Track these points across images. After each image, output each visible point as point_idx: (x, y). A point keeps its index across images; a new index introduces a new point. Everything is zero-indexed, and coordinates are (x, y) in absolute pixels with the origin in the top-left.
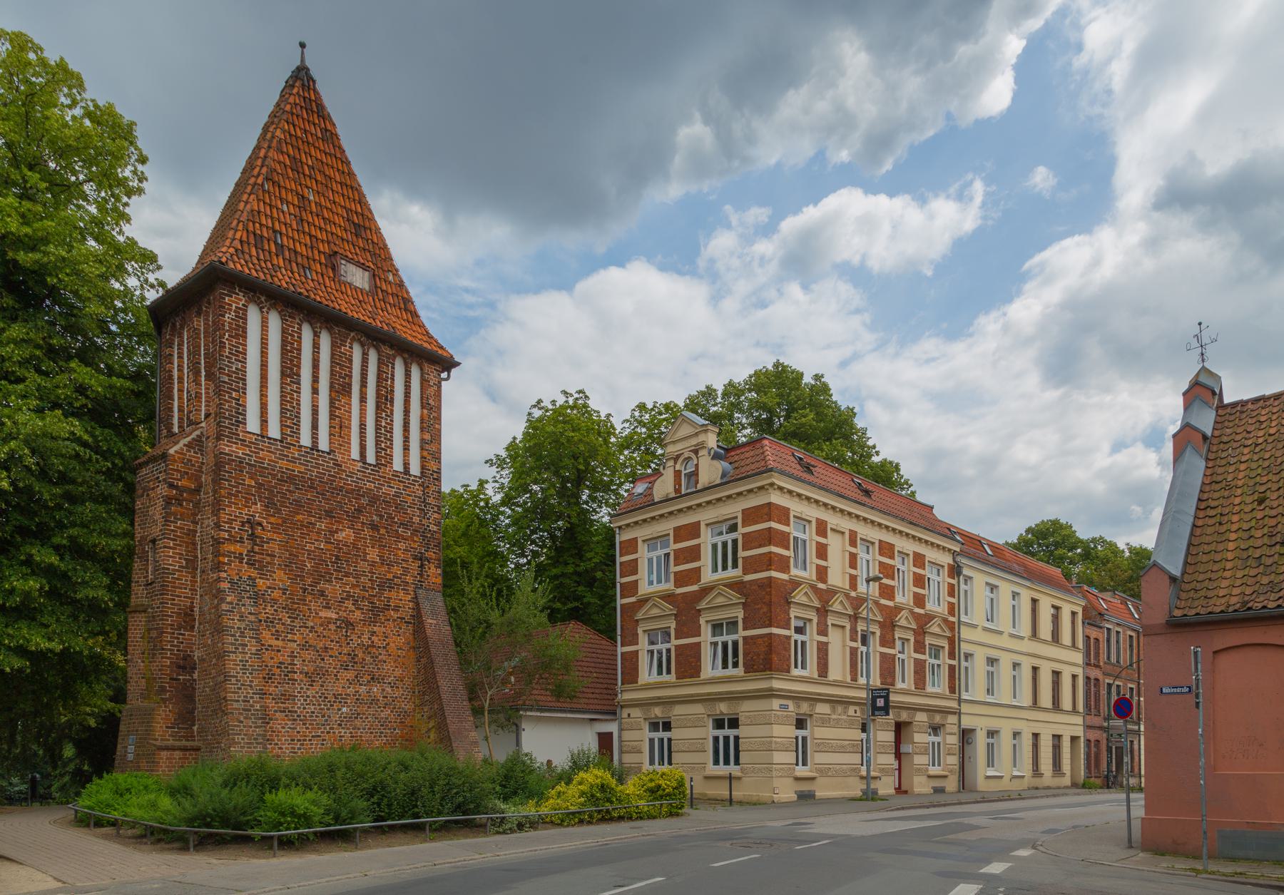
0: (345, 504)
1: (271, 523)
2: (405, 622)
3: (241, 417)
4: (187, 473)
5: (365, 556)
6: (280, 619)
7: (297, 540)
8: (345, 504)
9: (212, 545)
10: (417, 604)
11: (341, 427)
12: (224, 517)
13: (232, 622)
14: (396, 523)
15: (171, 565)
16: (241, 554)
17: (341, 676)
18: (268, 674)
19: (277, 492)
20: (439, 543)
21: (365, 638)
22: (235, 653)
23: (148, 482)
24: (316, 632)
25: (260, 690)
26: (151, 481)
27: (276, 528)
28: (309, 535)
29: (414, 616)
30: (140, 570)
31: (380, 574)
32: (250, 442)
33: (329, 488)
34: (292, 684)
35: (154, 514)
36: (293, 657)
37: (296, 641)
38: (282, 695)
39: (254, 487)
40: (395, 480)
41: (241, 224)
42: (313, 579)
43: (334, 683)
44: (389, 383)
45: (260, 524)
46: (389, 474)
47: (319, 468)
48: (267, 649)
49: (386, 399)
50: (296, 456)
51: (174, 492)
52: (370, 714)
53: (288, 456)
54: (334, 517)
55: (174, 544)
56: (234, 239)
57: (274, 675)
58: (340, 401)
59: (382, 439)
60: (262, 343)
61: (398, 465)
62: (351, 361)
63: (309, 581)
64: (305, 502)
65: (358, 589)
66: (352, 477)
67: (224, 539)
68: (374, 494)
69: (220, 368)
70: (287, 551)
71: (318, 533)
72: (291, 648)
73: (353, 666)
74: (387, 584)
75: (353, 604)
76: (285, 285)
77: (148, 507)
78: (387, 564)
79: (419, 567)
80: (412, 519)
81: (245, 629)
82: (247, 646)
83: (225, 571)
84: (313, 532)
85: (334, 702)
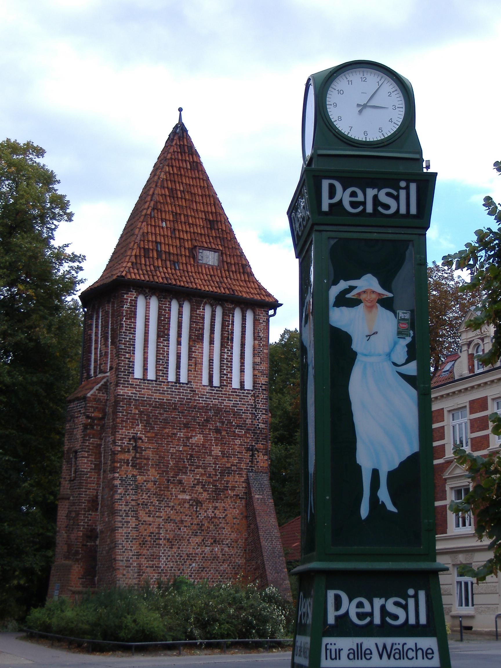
0: (197, 417)
2: (240, 498)
6: (152, 502)
7: (164, 447)
9: (111, 455)
10: (248, 484)
11: (196, 365)
12: (119, 436)
13: (121, 507)
14: (234, 426)
15: (85, 468)
16: (128, 460)
17: (192, 540)
18: (143, 541)
19: (153, 415)
20: (266, 437)
21: (210, 512)
22: (122, 527)
23: (74, 412)
24: (175, 510)
25: (137, 552)
26: (76, 412)
27: (150, 440)
28: (172, 442)
30: (67, 470)
31: (221, 464)
32: (136, 385)
33: (187, 407)
34: (159, 547)
35: (76, 434)
36: (159, 528)
37: (162, 517)
38: (151, 555)
39: (137, 414)
40: (233, 395)
41: (136, 245)
44: (230, 327)
45: (140, 438)
46: (229, 392)
47: (180, 395)
48: (142, 524)
49: (228, 339)
50: (165, 389)
52: (212, 568)
53: (160, 390)
54: (190, 427)
56: (131, 256)
57: (146, 541)
59: (225, 367)
60: (146, 319)
61: (236, 384)
62: (203, 318)
64: (170, 420)
65: (205, 476)
67: (118, 451)
68: (218, 407)
69: (120, 340)
70: (158, 454)
71: (179, 440)
74: (226, 471)
75: (201, 488)
76: (161, 280)
77: (73, 429)
78: (226, 457)
79: (250, 456)
80: (246, 421)
81: (129, 511)
82: (129, 522)
83: (118, 473)
84: (175, 439)
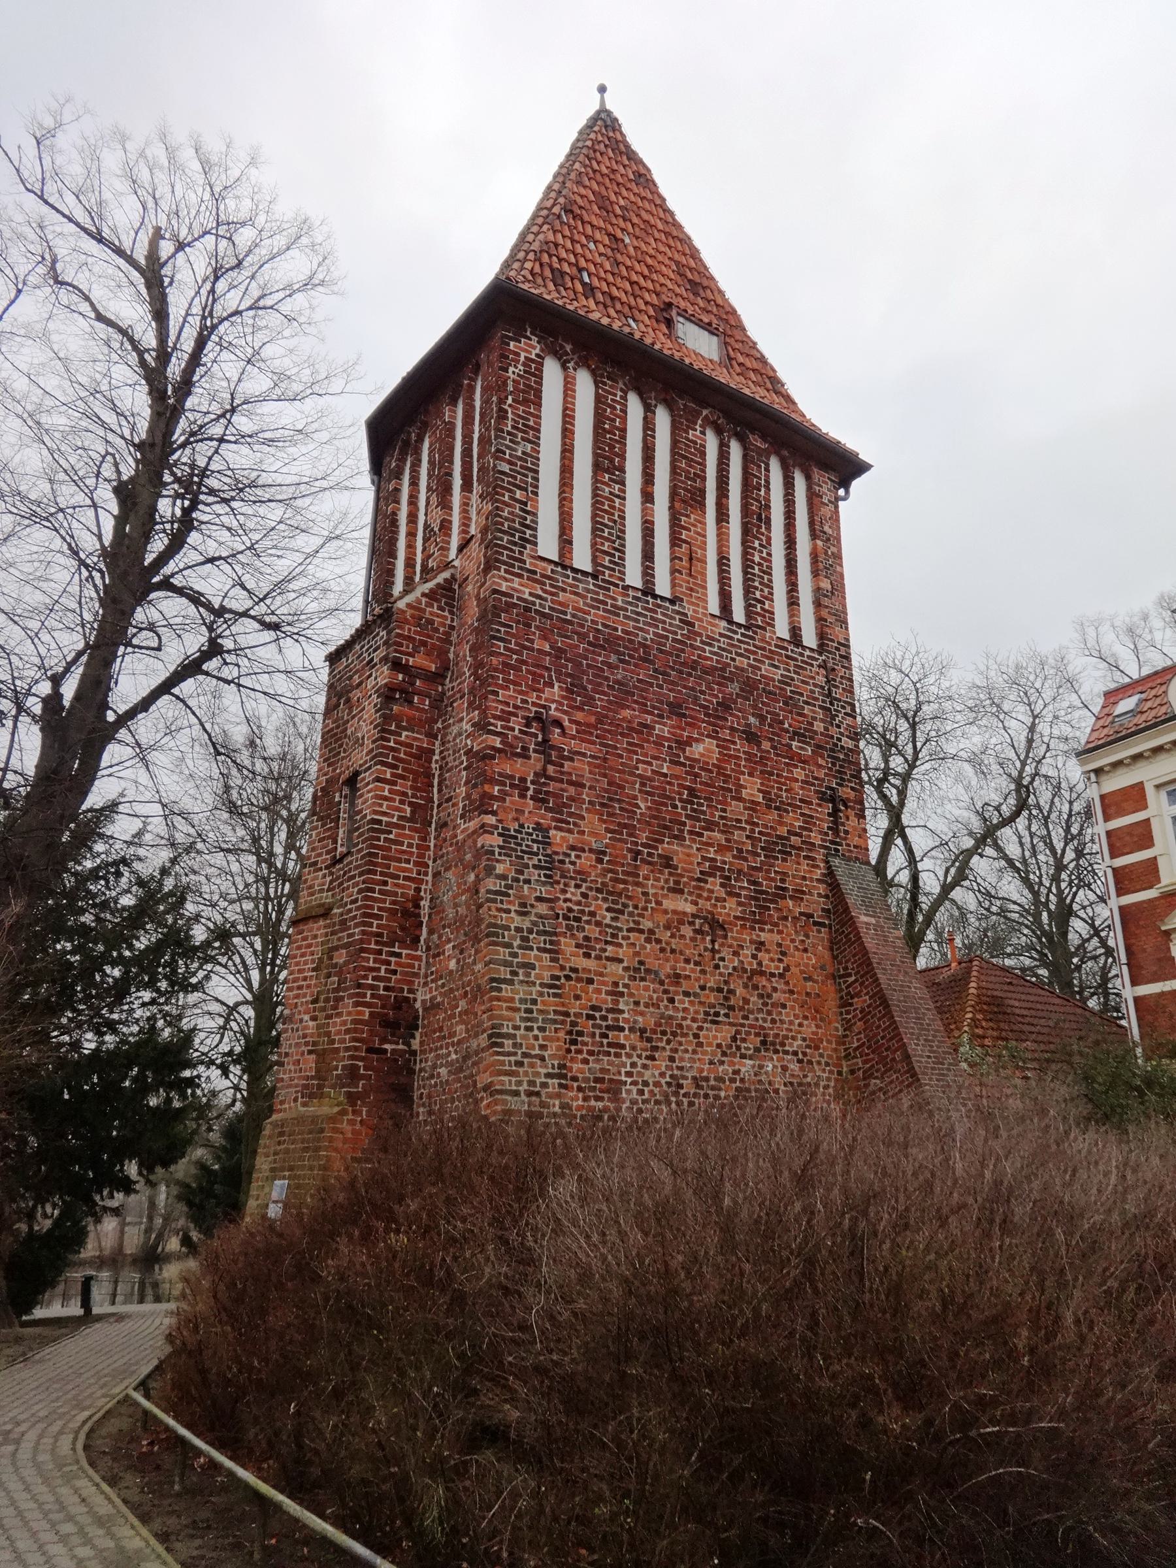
0: (702, 692)
1: (577, 723)
2: (816, 923)
3: (528, 532)
4: (424, 644)
5: (738, 791)
6: (593, 914)
7: (621, 756)
8: (702, 692)
14: (787, 731)
16: (523, 780)
21: (746, 956)
24: (658, 941)
27: (585, 732)
28: (642, 747)
29: (828, 911)
31: (766, 826)
32: (543, 576)
37: (621, 961)
38: (597, 1080)
39: (549, 654)
42: (651, 832)
43: (694, 1052)
45: (558, 723)
49: (760, 519)
50: (620, 603)
51: (400, 677)
54: (684, 715)
55: (393, 775)
57: (580, 1033)
58: (687, 516)
61: (782, 629)
62: (703, 454)
63: (643, 837)
64: (635, 687)
65: (729, 854)
66: (710, 645)
67: (493, 748)
70: (605, 775)
72: (612, 974)
73: (727, 1015)
74: (778, 848)
75: (722, 885)
78: (777, 808)
79: (829, 815)
81: (530, 931)
83: (494, 813)
84: (648, 741)
85: (695, 1095)
